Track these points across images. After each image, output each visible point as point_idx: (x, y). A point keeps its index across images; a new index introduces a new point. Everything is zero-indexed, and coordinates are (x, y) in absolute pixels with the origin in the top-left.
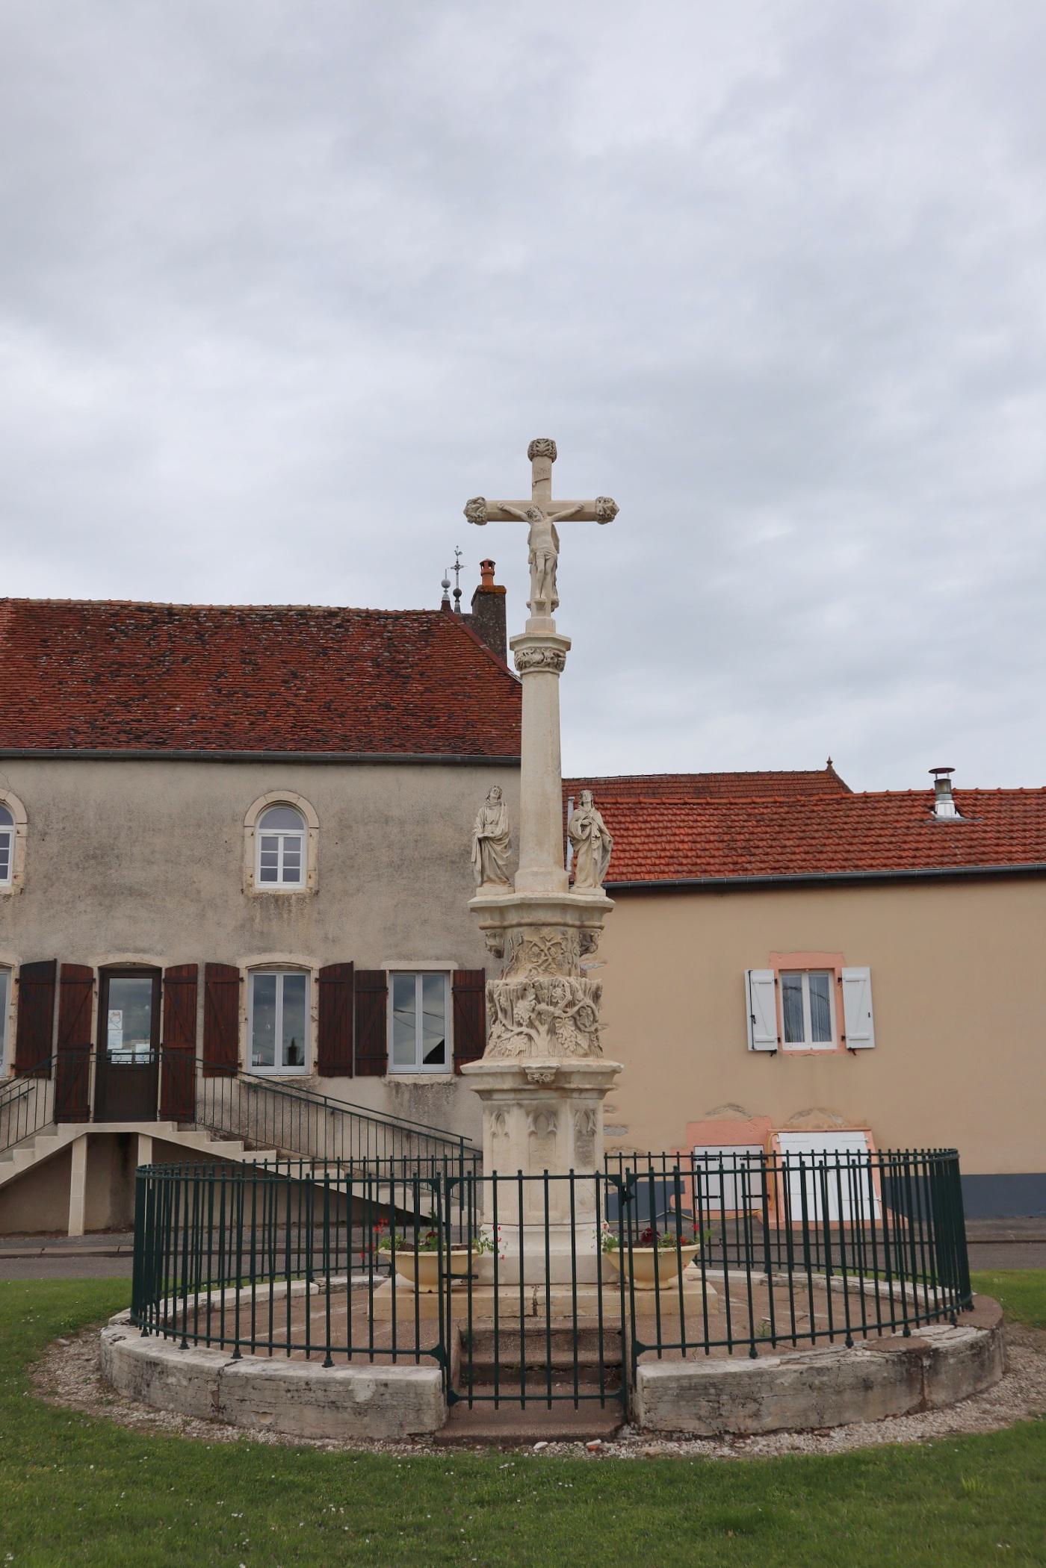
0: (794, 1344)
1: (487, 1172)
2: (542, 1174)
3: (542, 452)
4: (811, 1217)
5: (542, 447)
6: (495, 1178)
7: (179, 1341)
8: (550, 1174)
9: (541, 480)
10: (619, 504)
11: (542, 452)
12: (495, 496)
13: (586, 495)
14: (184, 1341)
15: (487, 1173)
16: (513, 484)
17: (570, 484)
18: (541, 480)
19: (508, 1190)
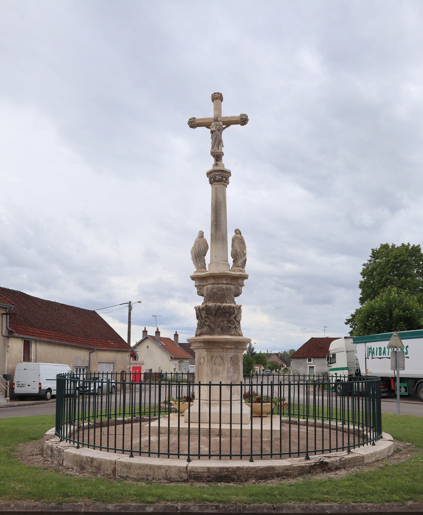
0: (281, 457)
1: (196, 382)
2: (219, 383)
3: (217, 98)
4: (153, 401)
5: (217, 95)
6: (200, 385)
7: (76, 444)
8: (201, 383)
9: (218, 109)
10: (249, 117)
11: (217, 98)
12: (199, 116)
13: (236, 114)
14: (78, 445)
15: (196, 382)
16: (207, 112)
17: (229, 110)
18: (218, 109)
19: (205, 390)
